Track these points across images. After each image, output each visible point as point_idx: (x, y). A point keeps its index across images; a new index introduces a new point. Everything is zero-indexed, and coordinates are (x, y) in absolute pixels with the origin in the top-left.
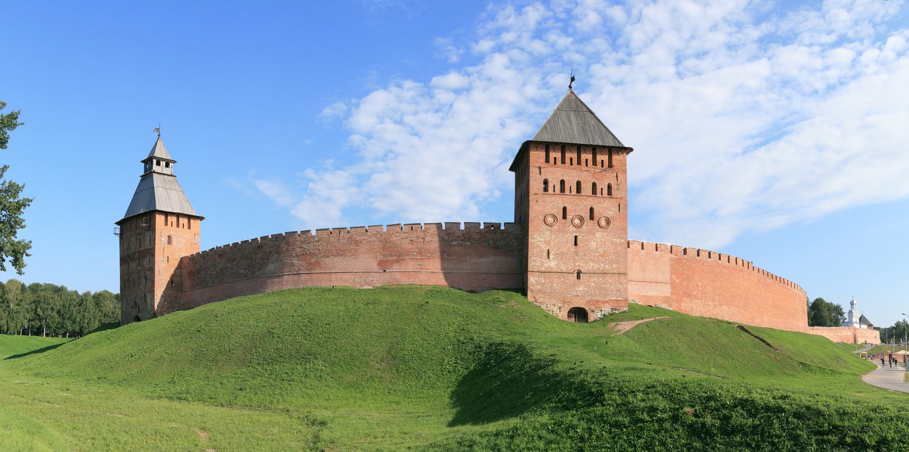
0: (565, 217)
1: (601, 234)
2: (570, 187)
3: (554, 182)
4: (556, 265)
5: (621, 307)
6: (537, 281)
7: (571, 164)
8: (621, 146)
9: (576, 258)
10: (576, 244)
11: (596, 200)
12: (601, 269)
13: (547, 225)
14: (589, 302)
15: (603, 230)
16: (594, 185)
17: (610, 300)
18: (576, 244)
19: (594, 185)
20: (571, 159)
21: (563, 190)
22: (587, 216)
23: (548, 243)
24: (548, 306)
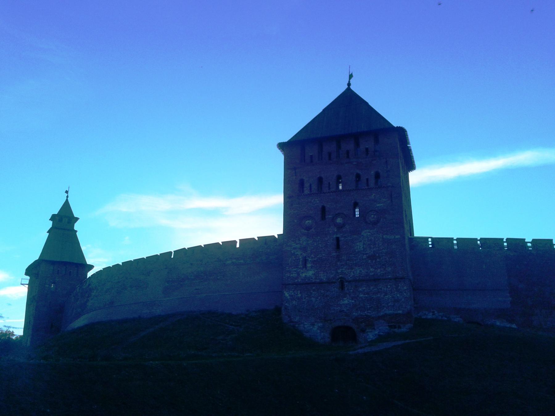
0: (323, 217)
1: (369, 232)
2: (329, 183)
4: (314, 274)
6: (291, 296)
7: (330, 158)
10: (338, 246)
16: (358, 176)
18: (338, 246)
19: (358, 176)
20: (330, 154)
23: (304, 249)
24: (306, 326)
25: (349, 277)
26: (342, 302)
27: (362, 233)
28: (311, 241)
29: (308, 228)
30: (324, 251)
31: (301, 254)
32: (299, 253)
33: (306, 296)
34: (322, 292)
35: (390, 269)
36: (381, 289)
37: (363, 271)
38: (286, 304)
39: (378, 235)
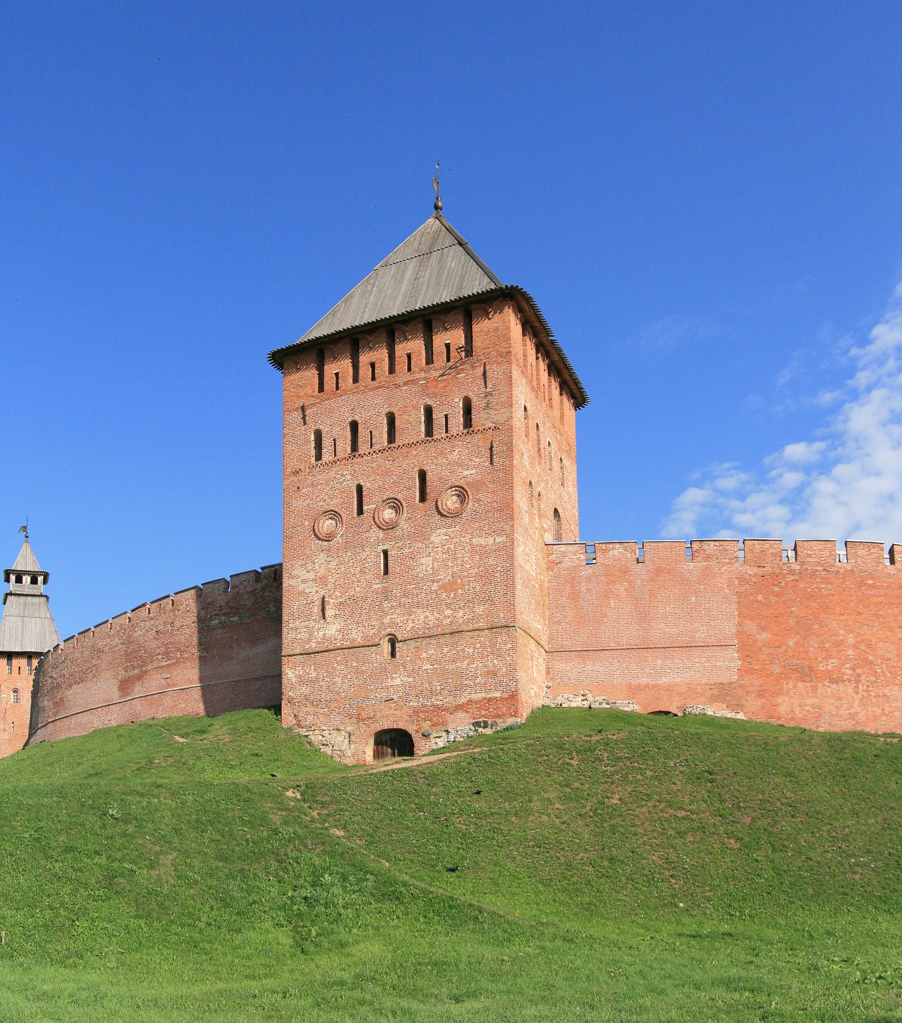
5: (499, 716)
6: (300, 677)
9: (386, 605)
11: (431, 448)
12: (445, 622)
13: (319, 539)
14: (416, 712)
15: (449, 521)
17: (470, 701)
19: (429, 411)
25: (405, 632)
27: (432, 538)
28: (335, 564)
30: (359, 581)
31: (317, 592)
33: (325, 675)
34: (355, 664)
35: (482, 608)
36: (463, 651)
37: (431, 617)
38: (290, 693)
39: (462, 539)
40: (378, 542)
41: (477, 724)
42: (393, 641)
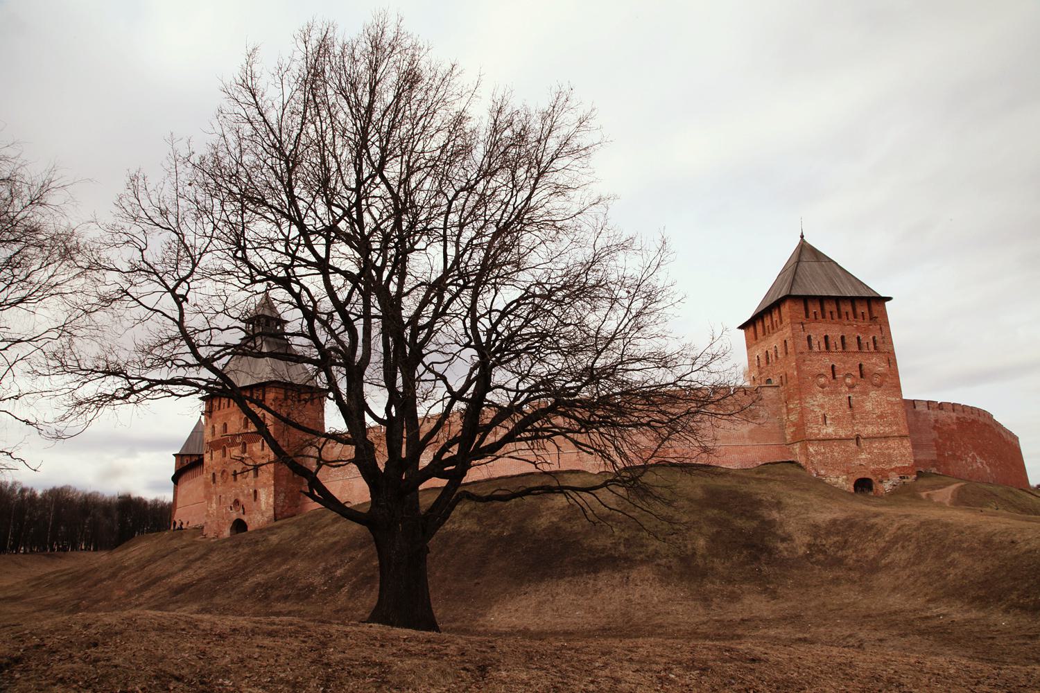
0: (834, 377)
3: (817, 340)
8: (874, 295)
10: (850, 407)
16: (858, 338)
21: (827, 347)
22: (858, 374)
23: (822, 406)
26: (860, 457)
29: (822, 386)
32: (817, 409)
40: (846, 393)
41: (901, 477)
42: (857, 439)
